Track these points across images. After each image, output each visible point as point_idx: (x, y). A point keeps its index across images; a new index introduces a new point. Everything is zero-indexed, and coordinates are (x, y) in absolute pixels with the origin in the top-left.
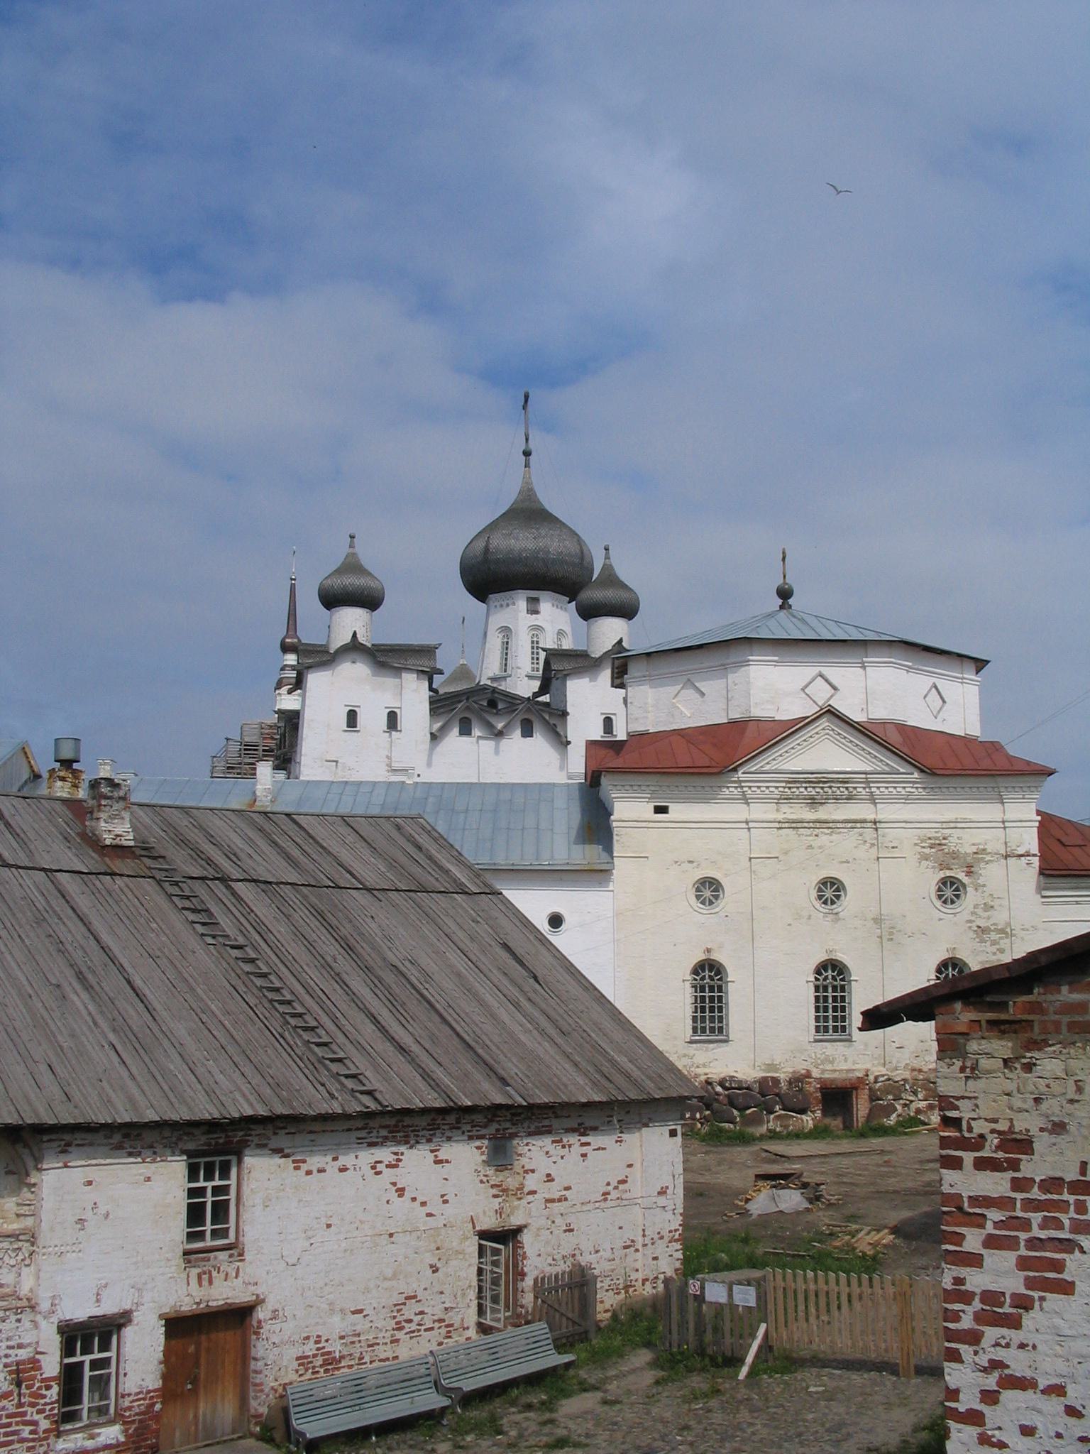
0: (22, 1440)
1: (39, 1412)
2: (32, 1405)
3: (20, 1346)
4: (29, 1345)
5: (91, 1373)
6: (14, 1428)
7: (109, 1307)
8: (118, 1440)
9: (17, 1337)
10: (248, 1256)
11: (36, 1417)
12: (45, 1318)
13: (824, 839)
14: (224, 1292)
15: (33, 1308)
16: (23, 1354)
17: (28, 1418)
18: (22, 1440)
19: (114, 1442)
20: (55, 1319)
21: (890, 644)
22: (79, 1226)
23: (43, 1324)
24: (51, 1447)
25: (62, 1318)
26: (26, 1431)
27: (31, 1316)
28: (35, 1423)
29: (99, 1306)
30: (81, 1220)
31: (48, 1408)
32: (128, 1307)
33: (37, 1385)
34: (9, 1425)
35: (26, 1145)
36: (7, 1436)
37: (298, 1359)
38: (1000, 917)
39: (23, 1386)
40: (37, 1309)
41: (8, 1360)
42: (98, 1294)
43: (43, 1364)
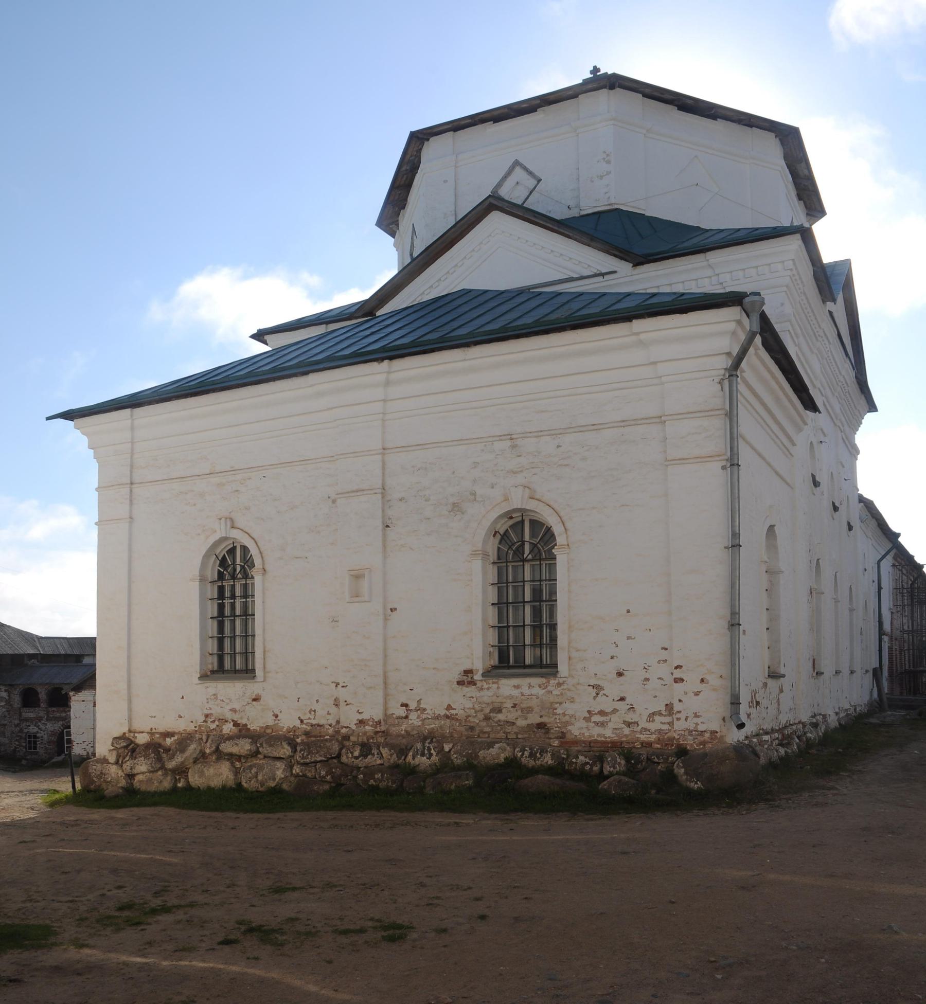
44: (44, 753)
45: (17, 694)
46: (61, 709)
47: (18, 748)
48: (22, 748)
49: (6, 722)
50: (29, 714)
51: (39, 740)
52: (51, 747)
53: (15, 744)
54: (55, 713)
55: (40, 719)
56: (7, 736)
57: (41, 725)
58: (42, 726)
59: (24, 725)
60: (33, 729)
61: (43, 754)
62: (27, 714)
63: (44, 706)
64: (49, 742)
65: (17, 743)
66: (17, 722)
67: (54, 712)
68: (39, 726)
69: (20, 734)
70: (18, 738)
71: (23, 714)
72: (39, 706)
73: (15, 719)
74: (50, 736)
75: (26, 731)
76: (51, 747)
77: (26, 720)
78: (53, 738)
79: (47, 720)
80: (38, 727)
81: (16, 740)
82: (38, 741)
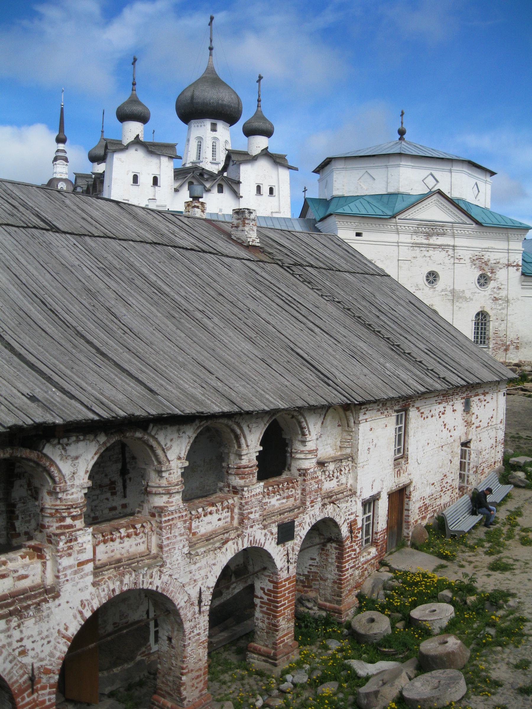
0: (352, 558)
1: (357, 544)
3: (352, 514)
7: (375, 492)
10: (409, 461)
13: (431, 253)
14: (403, 480)
18: (352, 558)
21: (463, 162)
28: (355, 550)
32: (379, 490)
34: (348, 552)
35: (352, 412)
37: (419, 508)
38: (503, 293)
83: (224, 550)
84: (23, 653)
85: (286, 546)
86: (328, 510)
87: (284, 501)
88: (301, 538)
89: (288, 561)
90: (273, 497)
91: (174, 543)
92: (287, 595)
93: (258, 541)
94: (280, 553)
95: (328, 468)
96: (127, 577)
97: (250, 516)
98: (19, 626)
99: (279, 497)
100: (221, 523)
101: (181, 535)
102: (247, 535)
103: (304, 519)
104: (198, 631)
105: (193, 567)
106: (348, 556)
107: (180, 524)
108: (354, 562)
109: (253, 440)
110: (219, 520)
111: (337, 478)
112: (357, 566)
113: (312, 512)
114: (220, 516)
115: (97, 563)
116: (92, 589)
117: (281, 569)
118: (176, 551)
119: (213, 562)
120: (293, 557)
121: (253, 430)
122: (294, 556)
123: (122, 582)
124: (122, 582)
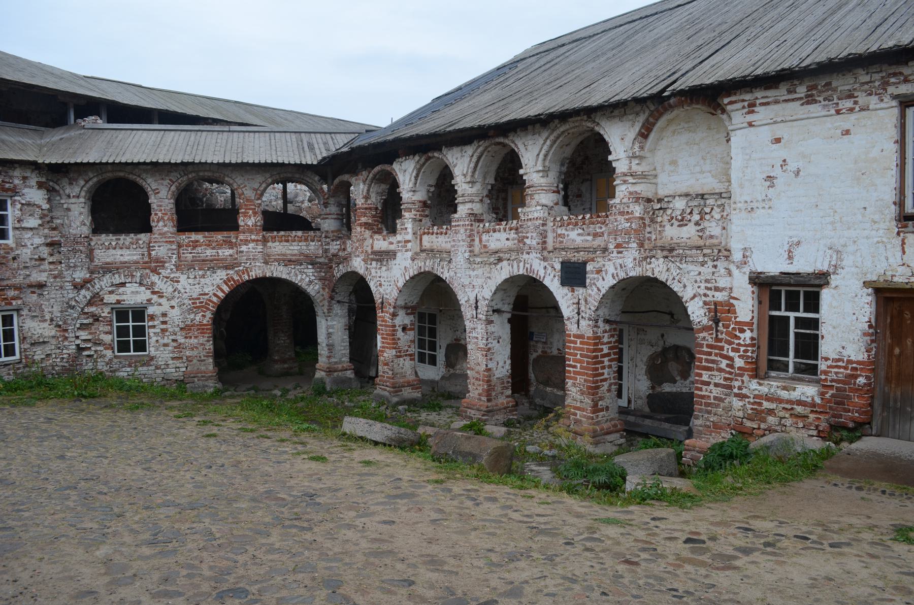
0: (720, 370)
2: (730, 343)
3: (717, 289)
4: (723, 289)
5: (796, 330)
6: (713, 357)
8: (813, 399)
9: (714, 281)
11: (731, 354)
12: (738, 267)
15: (727, 257)
16: (720, 297)
17: (725, 352)
18: (720, 370)
19: (809, 400)
20: (747, 270)
22: (768, 183)
23: (735, 272)
24: (745, 384)
25: (754, 270)
26: (724, 364)
27: (726, 264)
28: (731, 359)
29: (792, 263)
30: (770, 177)
31: (742, 349)
32: (825, 268)
33: (732, 326)
34: (710, 354)
36: (709, 363)
39: (720, 324)
40: (730, 258)
41: (707, 299)
42: (790, 251)
43: (737, 307)
44: (173, 359)
45: (78, 197)
46: (219, 236)
47: (89, 348)
48: (99, 348)
49: (42, 277)
50: (119, 252)
51: (156, 323)
52: (194, 341)
53: (77, 337)
54: (199, 249)
55: (155, 265)
56: (48, 317)
57: (159, 282)
58: (160, 285)
59: (104, 283)
60: (134, 296)
61: (170, 362)
62: (112, 252)
63: (166, 229)
64: (186, 329)
65: (84, 335)
66: (80, 275)
67: (195, 244)
68: (153, 284)
69: (92, 309)
70: (85, 321)
71: (97, 252)
72: (148, 229)
73: (75, 266)
74: (190, 311)
75: (112, 299)
76: (194, 341)
77: (108, 269)
78: (198, 318)
79: (178, 267)
80: (151, 287)
81: (83, 327)
82: (154, 327)
83: (498, 267)
84: (380, 285)
85: (576, 293)
86: (652, 266)
87: (590, 238)
88: (599, 290)
89: (578, 314)
90: (573, 230)
91: (458, 246)
92: (578, 356)
93: (536, 272)
94: (566, 298)
95: (671, 205)
96: (428, 261)
97: (525, 240)
98: (380, 268)
99: (580, 231)
100: (509, 244)
101: (464, 241)
102: (523, 260)
103: (604, 265)
104: (476, 336)
105: (471, 273)
106: (707, 361)
107: (462, 230)
108: (726, 379)
109: (530, 158)
110: (508, 239)
111: (697, 224)
112: (736, 391)
113: (620, 261)
114: (508, 236)
115: (424, 247)
116: (410, 261)
117: (569, 319)
118: (459, 254)
119: (489, 275)
120: (588, 312)
121: (529, 148)
122: (588, 311)
123: (425, 263)
124: (425, 263)
